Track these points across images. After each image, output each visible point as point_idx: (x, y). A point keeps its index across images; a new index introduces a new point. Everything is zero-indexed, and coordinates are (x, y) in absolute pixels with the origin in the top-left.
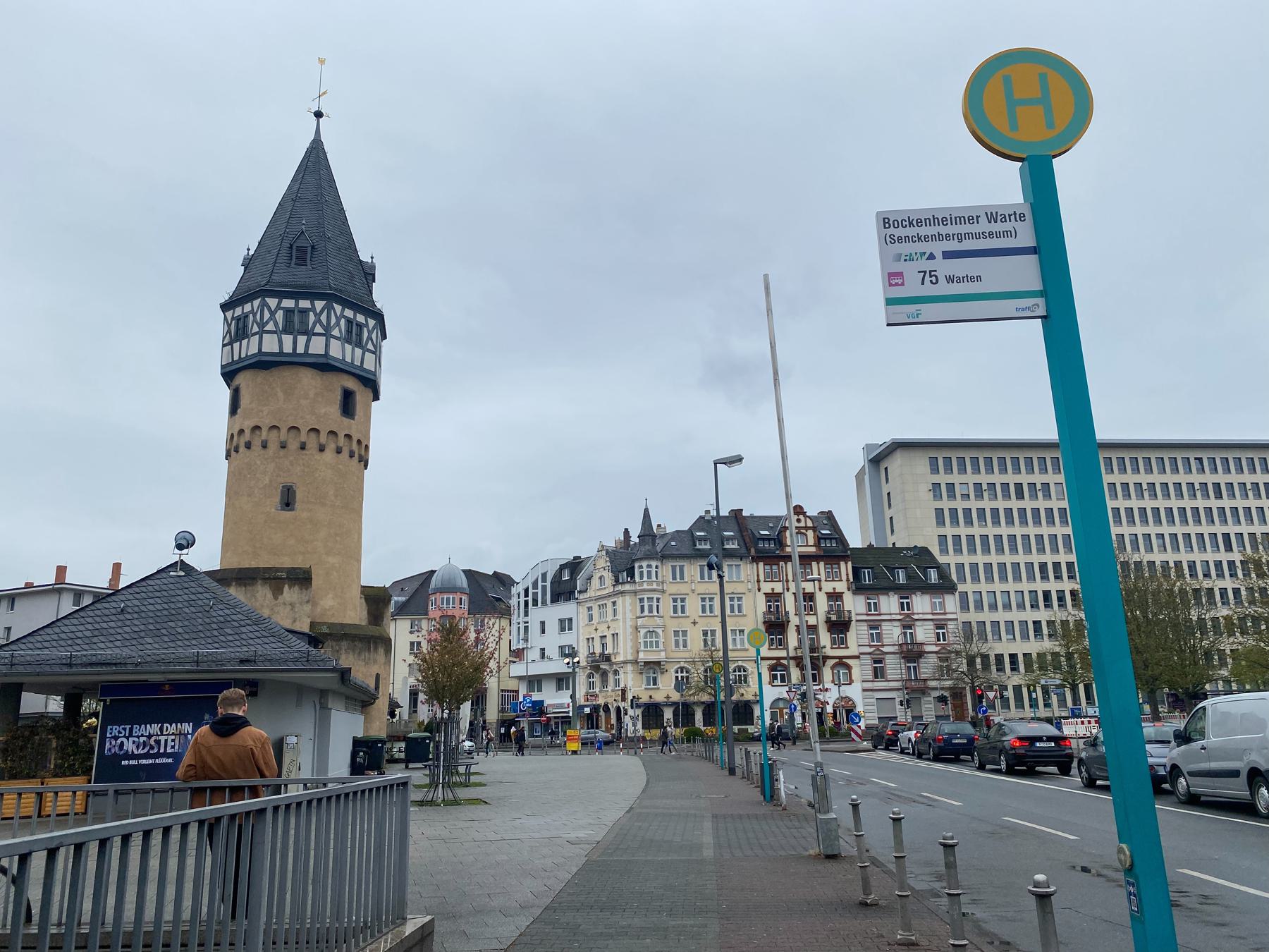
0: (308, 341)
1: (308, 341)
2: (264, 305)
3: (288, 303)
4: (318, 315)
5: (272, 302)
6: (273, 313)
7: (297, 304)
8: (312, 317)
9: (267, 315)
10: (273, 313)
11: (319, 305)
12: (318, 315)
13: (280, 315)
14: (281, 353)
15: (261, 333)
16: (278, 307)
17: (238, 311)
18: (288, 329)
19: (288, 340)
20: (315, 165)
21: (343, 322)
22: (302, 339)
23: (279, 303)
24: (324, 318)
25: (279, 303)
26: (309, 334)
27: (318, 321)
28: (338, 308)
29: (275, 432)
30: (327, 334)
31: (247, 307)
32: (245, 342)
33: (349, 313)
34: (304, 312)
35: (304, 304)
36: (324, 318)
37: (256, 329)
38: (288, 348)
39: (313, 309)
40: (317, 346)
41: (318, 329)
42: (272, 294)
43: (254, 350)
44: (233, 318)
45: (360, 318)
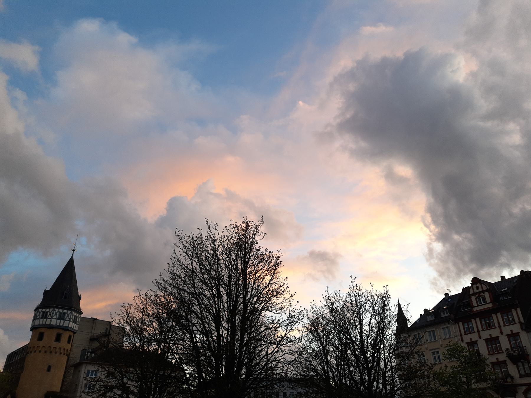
0: (64, 322)
1: (64, 322)
3: (61, 310)
5: (57, 310)
6: (56, 313)
8: (66, 315)
9: (54, 314)
10: (56, 313)
11: (69, 312)
12: (68, 315)
13: (58, 314)
16: (58, 311)
17: (44, 310)
18: (59, 318)
19: (58, 321)
20: (71, 263)
22: (62, 321)
30: (69, 321)
31: (48, 310)
32: (45, 320)
33: (75, 314)
34: (65, 313)
35: (65, 311)
37: (50, 317)
38: (58, 324)
40: (66, 324)
42: (57, 308)
45: (77, 315)
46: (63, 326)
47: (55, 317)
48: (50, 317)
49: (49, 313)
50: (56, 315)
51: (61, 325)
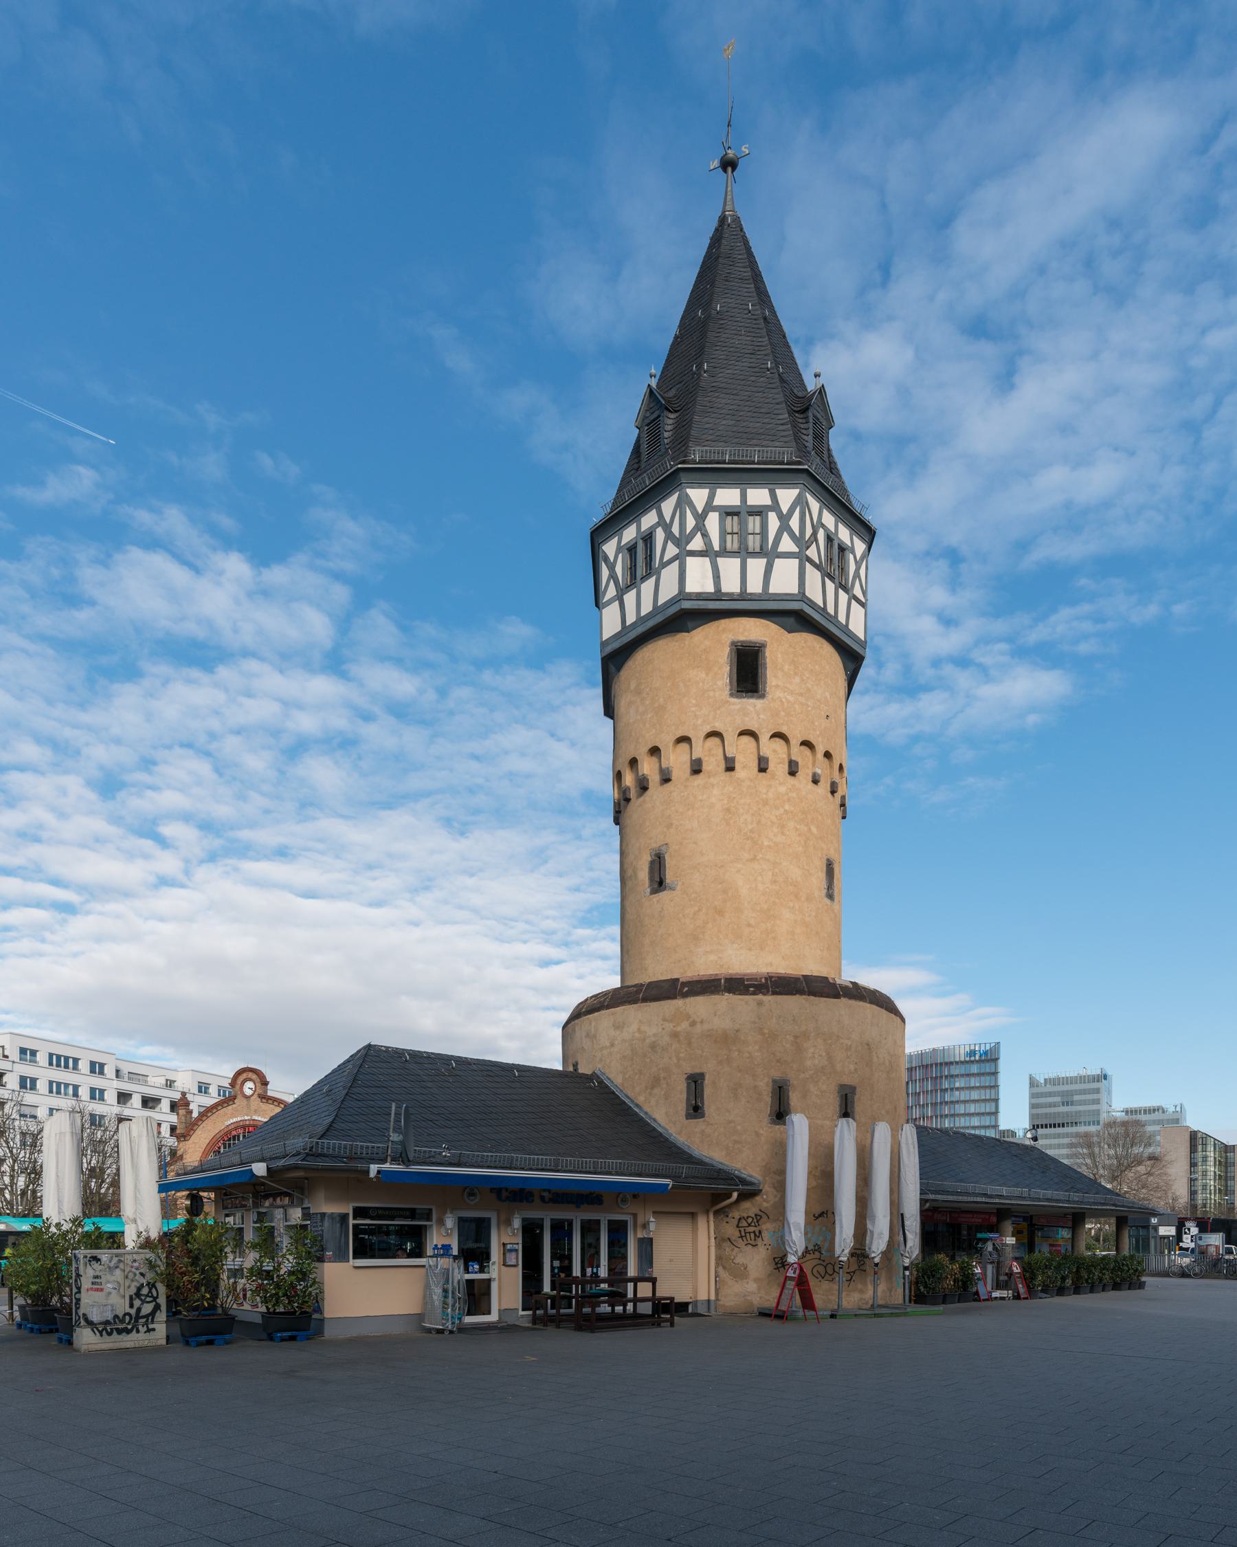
2: (684, 502)
3: (728, 496)
4: (784, 519)
5: (698, 496)
6: (701, 518)
7: (744, 497)
8: (773, 522)
9: (691, 522)
11: (787, 496)
12: (784, 519)
14: (718, 595)
15: (680, 558)
17: (629, 534)
19: (730, 567)
21: (821, 535)
22: (756, 566)
23: (711, 497)
24: (794, 523)
25: (711, 497)
26: (770, 554)
27: (784, 527)
28: (814, 505)
29: (685, 746)
31: (649, 520)
35: (758, 496)
36: (794, 523)
38: (731, 585)
39: (775, 506)
40: (785, 578)
41: (787, 545)
43: (668, 590)
44: (619, 549)
46: (765, 596)
47: (697, 543)
48: (672, 550)
49: (660, 535)
50: (700, 527)
51: (754, 587)
